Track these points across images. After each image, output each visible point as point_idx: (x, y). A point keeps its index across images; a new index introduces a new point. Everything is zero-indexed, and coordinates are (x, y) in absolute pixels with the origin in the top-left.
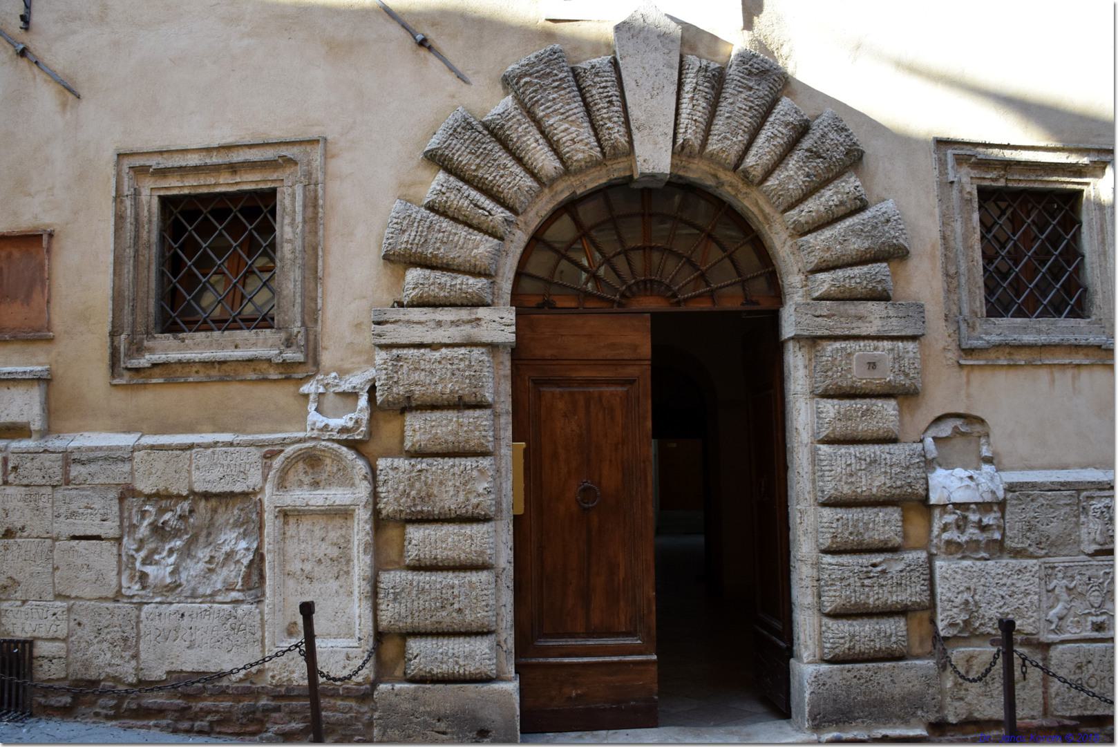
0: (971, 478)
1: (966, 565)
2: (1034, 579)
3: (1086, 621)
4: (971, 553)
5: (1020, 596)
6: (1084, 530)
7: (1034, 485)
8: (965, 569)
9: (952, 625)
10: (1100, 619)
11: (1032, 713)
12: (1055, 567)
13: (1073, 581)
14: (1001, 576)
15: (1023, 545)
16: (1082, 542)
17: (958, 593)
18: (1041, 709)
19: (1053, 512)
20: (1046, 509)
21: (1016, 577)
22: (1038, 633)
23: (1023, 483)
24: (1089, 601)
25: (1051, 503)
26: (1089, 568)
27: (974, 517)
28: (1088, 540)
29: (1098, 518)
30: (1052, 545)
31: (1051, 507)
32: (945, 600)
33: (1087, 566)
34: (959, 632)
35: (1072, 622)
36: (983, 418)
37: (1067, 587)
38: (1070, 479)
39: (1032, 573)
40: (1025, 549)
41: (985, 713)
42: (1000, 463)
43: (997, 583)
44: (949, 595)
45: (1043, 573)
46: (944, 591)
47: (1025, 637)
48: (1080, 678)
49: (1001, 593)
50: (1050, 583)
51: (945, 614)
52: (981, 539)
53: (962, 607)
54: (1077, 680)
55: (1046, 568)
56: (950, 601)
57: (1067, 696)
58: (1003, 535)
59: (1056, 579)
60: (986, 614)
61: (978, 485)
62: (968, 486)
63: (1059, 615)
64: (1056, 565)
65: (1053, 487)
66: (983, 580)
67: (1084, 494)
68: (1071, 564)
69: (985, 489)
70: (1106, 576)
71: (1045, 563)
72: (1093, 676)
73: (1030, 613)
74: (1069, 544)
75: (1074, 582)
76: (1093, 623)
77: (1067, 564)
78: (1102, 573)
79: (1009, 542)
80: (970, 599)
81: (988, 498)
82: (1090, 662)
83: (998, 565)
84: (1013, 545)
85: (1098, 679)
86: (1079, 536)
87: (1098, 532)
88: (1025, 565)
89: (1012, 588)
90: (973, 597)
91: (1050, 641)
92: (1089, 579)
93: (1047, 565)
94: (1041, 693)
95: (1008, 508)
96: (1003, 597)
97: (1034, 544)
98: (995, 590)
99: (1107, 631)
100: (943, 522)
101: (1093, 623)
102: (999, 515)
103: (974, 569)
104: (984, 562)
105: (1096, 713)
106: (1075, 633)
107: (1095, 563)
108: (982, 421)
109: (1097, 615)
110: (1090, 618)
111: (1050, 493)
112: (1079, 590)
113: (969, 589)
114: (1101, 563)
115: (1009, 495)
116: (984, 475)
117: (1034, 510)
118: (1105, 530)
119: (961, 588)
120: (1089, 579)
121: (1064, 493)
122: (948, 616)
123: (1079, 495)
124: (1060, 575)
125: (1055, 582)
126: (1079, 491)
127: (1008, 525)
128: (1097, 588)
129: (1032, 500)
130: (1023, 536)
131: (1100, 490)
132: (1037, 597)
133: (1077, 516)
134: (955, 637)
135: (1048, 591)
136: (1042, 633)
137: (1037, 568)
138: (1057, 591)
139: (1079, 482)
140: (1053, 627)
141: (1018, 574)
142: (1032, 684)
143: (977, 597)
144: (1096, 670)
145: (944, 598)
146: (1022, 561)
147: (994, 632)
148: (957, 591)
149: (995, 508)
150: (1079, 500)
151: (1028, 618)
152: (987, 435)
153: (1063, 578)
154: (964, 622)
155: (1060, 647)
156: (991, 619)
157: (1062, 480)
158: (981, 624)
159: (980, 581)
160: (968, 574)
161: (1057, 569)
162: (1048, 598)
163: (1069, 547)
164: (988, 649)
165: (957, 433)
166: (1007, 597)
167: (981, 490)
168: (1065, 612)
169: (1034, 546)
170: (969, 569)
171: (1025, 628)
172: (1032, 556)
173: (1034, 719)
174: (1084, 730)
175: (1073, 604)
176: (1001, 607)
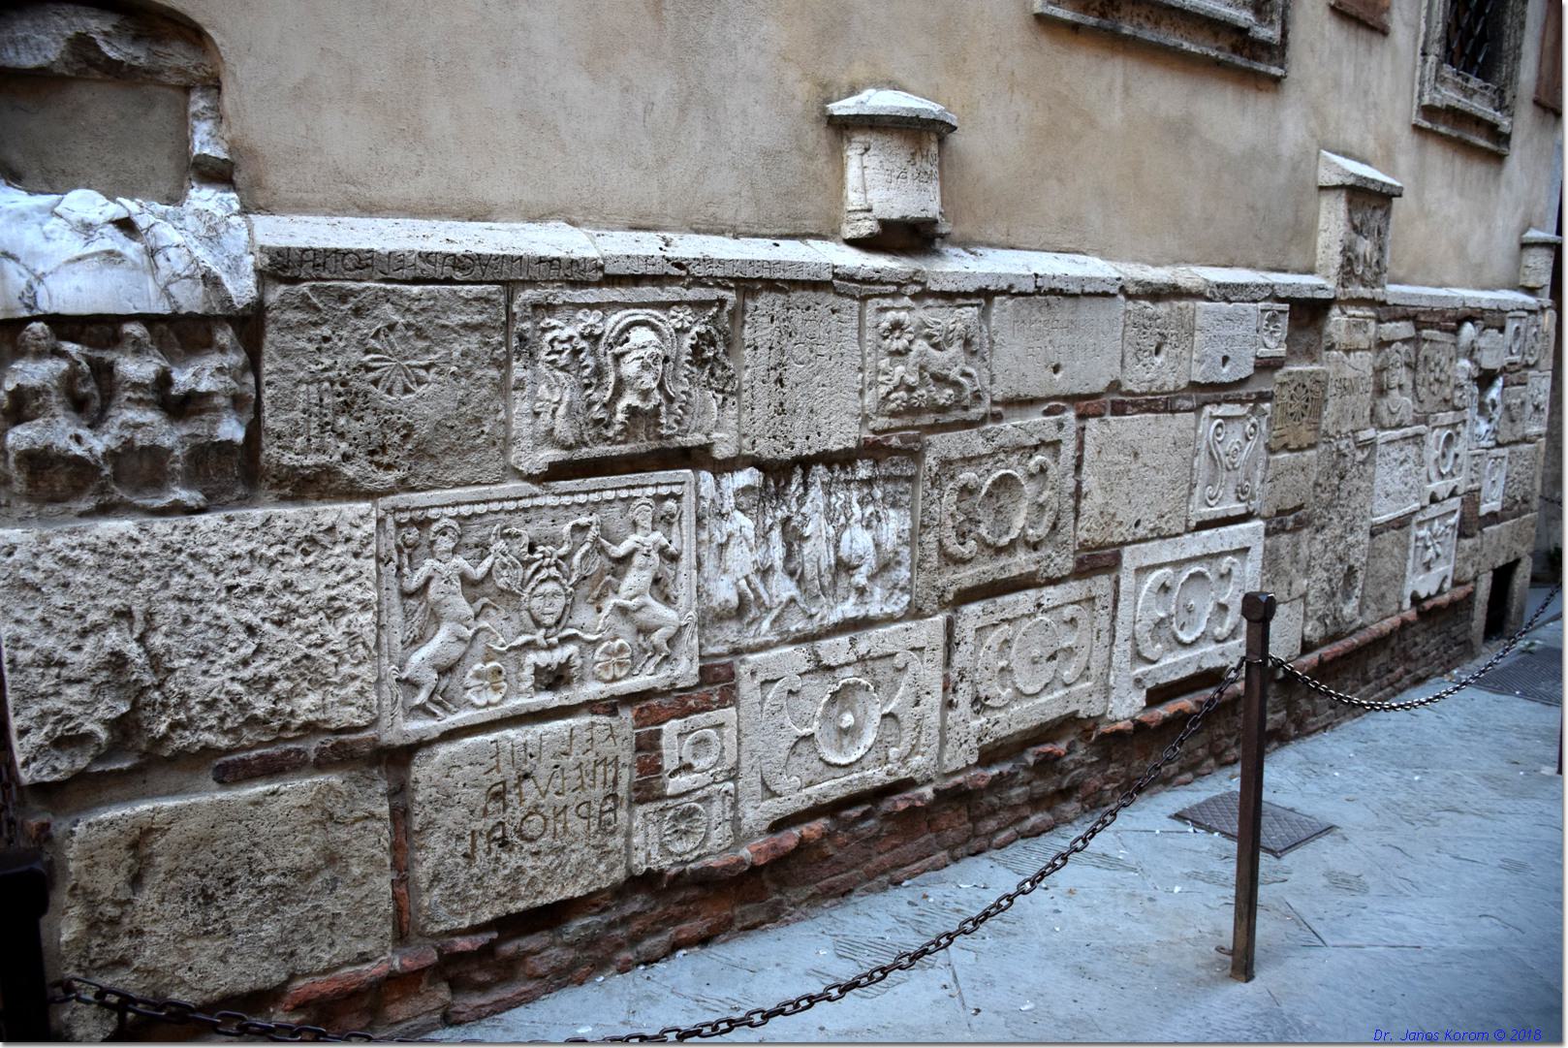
0: (126, 225)
1: (112, 535)
2: (361, 561)
3: (521, 667)
4: (137, 491)
5: (313, 620)
6: (521, 406)
7: (363, 262)
8: (107, 552)
9: (67, 741)
10: (559, 655)
11: (361, 947)
12: (429, 522)
13: (482, 558)
14: (245, 564)
15: (324, 459)
16: (514, 441)
17: (84, 634)
18: (389, 929)
19: (428, 350)
20: (404, 339)
21: (297, 561)
22: (373, 723)
23: (326, 253)
24: (529, 610)
25: (420, 321)
26: (532, 515)
27: (136, 368)
28: (532, 437)
29: (562, 369)
30: (421, 453)
31: (420, 333)
32: (33, 663)
33: (525, 510)
34: (98, 759)
35: (478, 675)
36: (199, 18)
37: (463, 577)
38: (486, 249)
39: (354, 546)
40: (328, 471)
41: (209, 985)
42: (257, 183)
43: (230, 589)
44: (49, 642)
45: (389, 542)
46: (24, 631)
47: (333, 739)
48: (501, 823)
49: (247, 616)
50: (413, 570)
51: (35, 710)
52: (167, 442)
53: (103, 676)
54: (493, 830)
55: (399, 525)
56: (49, 662)
57: (462, 877)
58: (254, 430)
59: (432, 555)
60: (193, 691)
61: (152, 253)
62: (112, 256)
63: (440, 661)
64: (432, 513)
65: (429, 270)
66: (178, 581)
67: (528, 294)
68: (480, 509)
69: (179, 268)
70: (578, 537)
71: (396, 510)
72: (535, 809)
73: (345, 669)
74: (473, 448)
75: (487, 562)
76: (538, 670)
77: (465, 510)
78: (567, 527)
79: (273, 451)
80: (133, 650)
81: (191, 299)
82: (526, 776)
83: (232, 528)
84: (289, 459)
85: (550, 814)
86: (506, 423)
87: (562, 410)
88: (327, 520)
89: (287, 598)
90: (141, 640)
91: (413, 739)
92: (532, 549)
93: (405, 517)
94: (388, 887)
95: (271, 335)
96: (251, 630)
97: (361, 454)
98: (222, 609)
99: (575, 685)
100: (10, 386)
101: (538, 670)
102: (236, 358)
103: (143, 548)
104: (183, 521)
105: (540, 901)
106: (488, 704)
107: (551, 500)
108: (194, 35)
109: (550, 647)
110: (532, 658)
111: (416, 289)
112: (501, 583)
113: (125, 615)
114: (566, 500)
115: (275, 293)
116: (190, 221)
117: (361, 342)
118: (580, 404)
119: (95, 617)
120: (532, 549)
121: (464, 290)
122: (43, 715)
123: (510, 300)
124: (445, 543)
125: (428, 565)
126: (510, 286)
127: (268, 392)
128: (553, 571)
129: (357, 312)
130: (322, 427)
131: (575, 284)
132: (369, 617)
133: (503, 365)
134: (80, 777)
135: (406, 595)
136: (385, 722)
137: (370, 527)
138: (433, 593)
139: (512, 259)
140: (422, 696)
141: (306, 553)
142: (356, 871)
143: (157, 640)
144: (544, 794)
145: (24, 656)
146: (319, 508)
147: (224, 742)
148: (76, 626)
149: (225, 336)
150: (511, 315)
151: (342, 685)
152: (213, 85)
153: (454, 551)
154: (117, 725)
155: (444, 751)
156: (211, 705)
157: (457, 249)
158: (174, 726)
159: (166, 586)
160: (118, 564)
161: (435, 527)
162: (408, 615)
163: (474, 457)
164: (204, 799)
165: (91, 63)
166: (267, 626)
167: (165, 271)
168: (457, 650)
169: (362, 459)
170: (127, 547)
171: (331, 713)
172: (353, 492)
173: (368, 961)
174: (509, 948)
175: (483, 623)
176: (245, 663)
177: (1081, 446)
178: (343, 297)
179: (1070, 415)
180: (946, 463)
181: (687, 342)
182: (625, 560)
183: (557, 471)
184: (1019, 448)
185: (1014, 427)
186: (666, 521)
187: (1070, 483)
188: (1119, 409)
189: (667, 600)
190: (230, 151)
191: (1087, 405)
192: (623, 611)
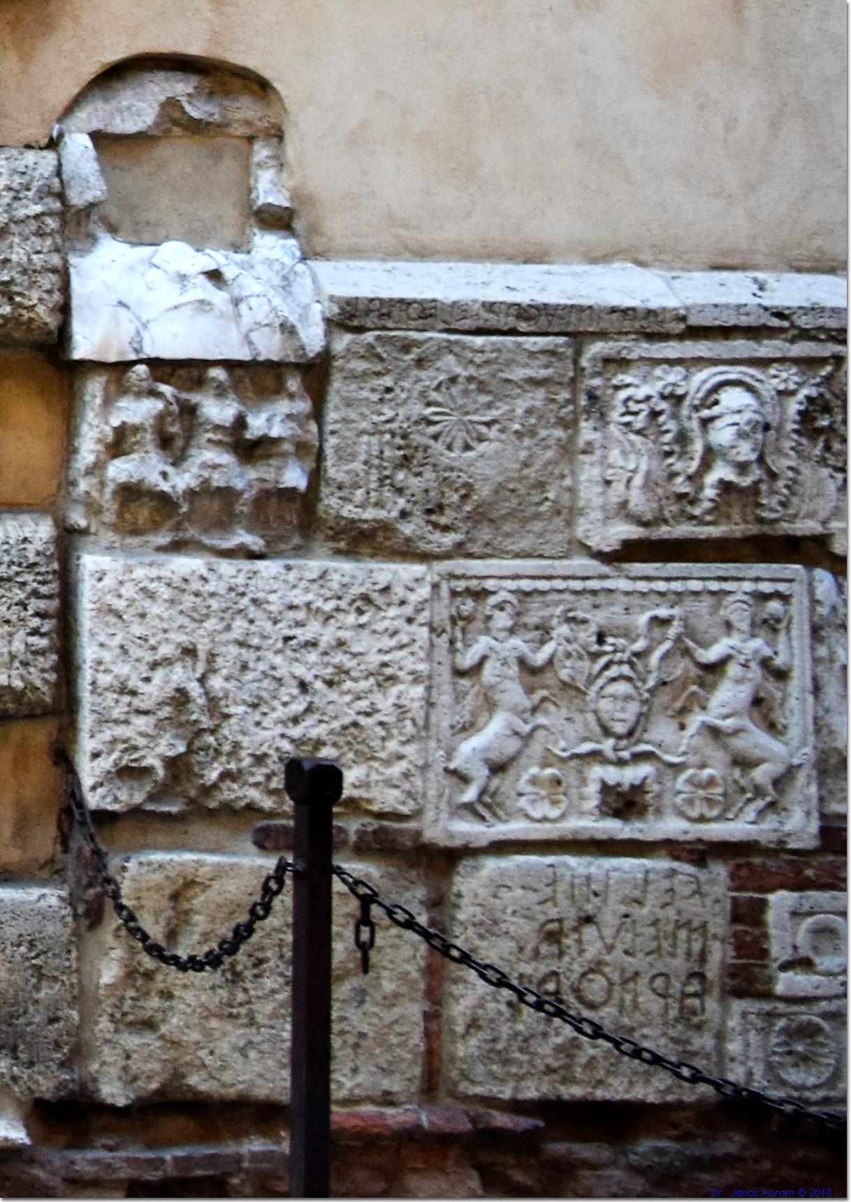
7: (427, 312)
31: (482, 387)
40: (384, 527)
67: (597, 348)
84: (348, 511)
129: (420, 363)
152: (277, 135)
178: (406, 347)
181: (793, 407)
182: (716, 669)
183: (629, 552)
186: (771, 626)
189: (772, 728)
190: (292, 199)
192: (714, 732)
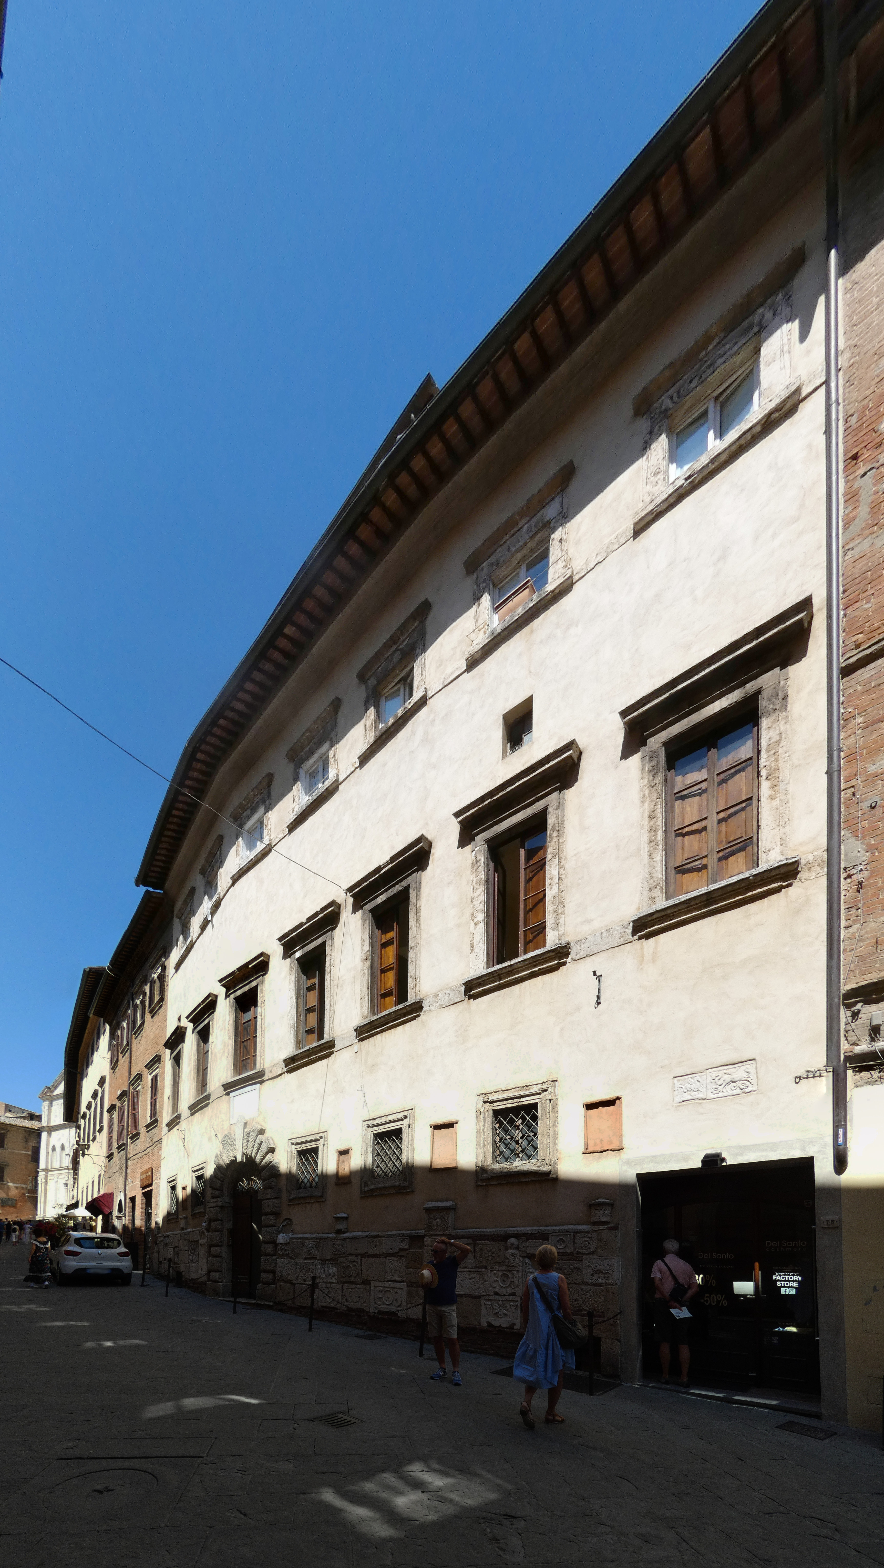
177: (361, 1262)
179: (359, 1257)
180: (341, 1262)
184: (351, 1261)
185: (350, 1258)
187: (360, 1268)
188: (368, 1257)
191: (363, 1256)
